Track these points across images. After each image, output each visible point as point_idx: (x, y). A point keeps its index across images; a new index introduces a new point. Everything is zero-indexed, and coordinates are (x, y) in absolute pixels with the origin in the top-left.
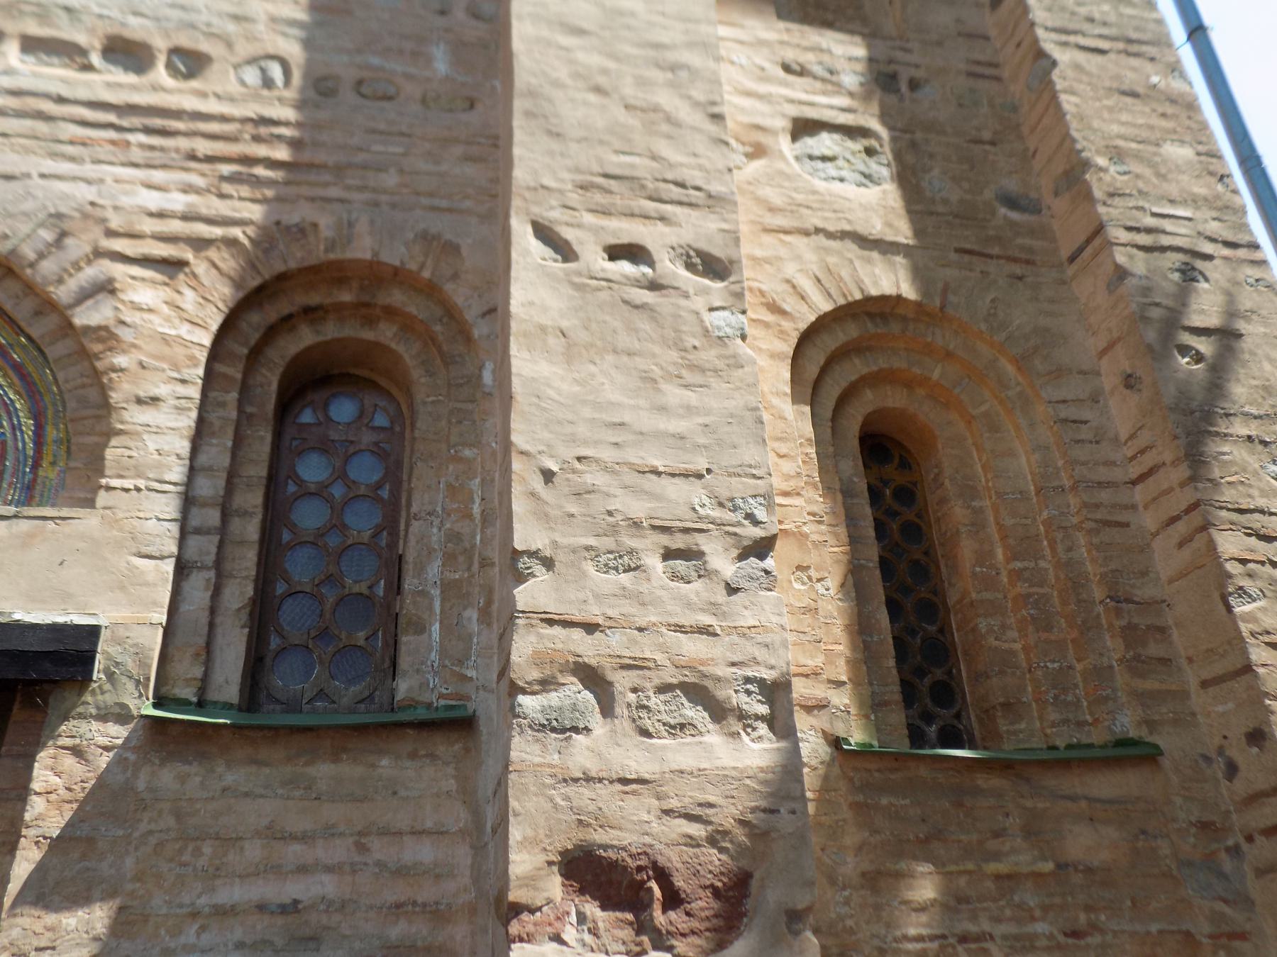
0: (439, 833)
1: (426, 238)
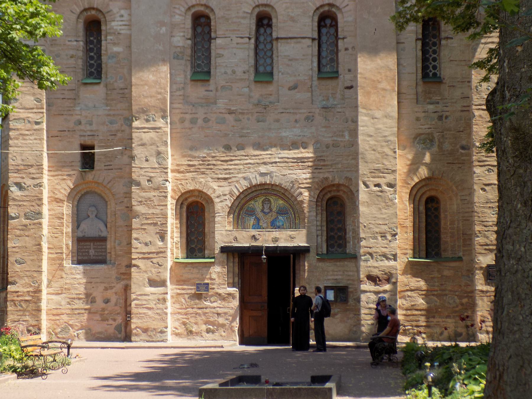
0: (353, 271)
1: (346, 178)
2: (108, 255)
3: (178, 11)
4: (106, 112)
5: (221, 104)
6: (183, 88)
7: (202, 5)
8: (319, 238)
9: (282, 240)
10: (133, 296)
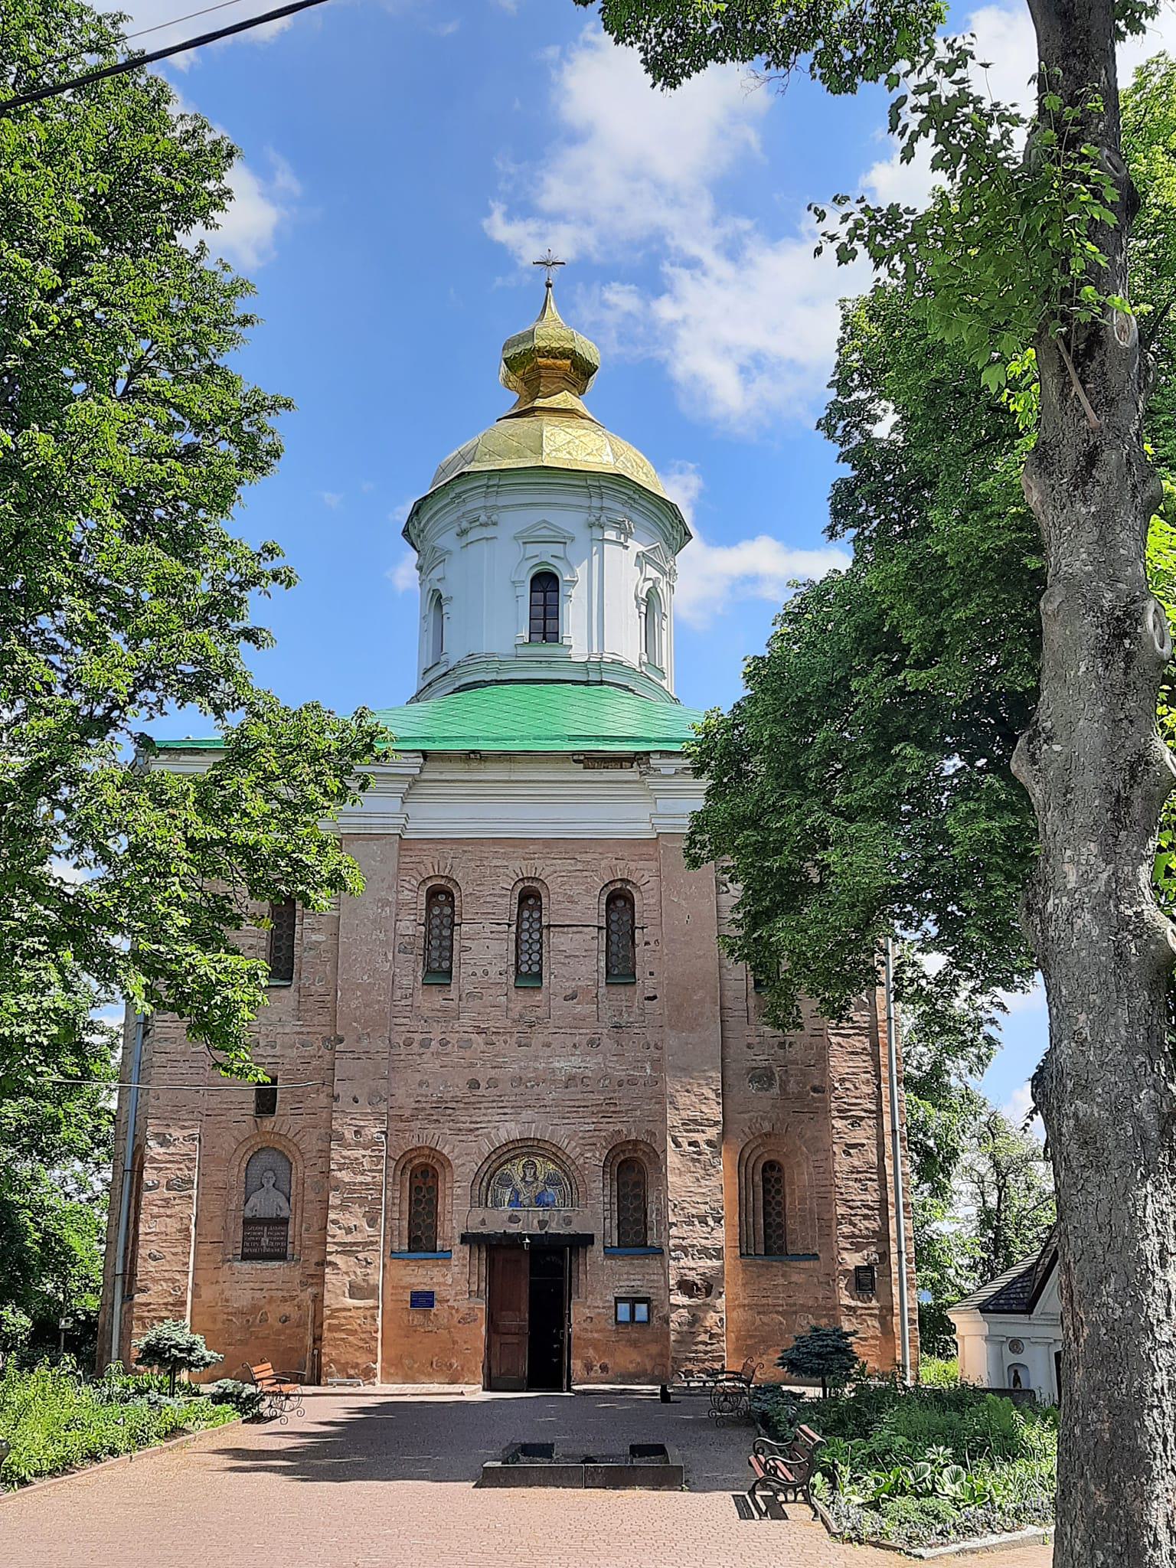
2: (290, 1246)
3: (407, 885)
4: (298, 1029)
5: (466, 1020)
6: (412, 995)
7: (442, 877)
8: (608, 1221)
9: (554, 1225)
10: (327, 1312)
